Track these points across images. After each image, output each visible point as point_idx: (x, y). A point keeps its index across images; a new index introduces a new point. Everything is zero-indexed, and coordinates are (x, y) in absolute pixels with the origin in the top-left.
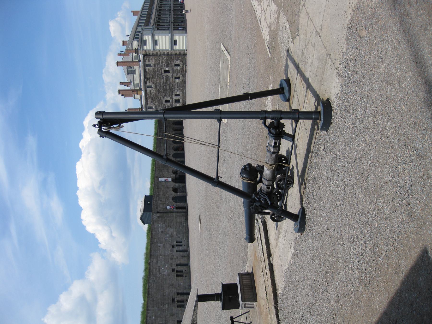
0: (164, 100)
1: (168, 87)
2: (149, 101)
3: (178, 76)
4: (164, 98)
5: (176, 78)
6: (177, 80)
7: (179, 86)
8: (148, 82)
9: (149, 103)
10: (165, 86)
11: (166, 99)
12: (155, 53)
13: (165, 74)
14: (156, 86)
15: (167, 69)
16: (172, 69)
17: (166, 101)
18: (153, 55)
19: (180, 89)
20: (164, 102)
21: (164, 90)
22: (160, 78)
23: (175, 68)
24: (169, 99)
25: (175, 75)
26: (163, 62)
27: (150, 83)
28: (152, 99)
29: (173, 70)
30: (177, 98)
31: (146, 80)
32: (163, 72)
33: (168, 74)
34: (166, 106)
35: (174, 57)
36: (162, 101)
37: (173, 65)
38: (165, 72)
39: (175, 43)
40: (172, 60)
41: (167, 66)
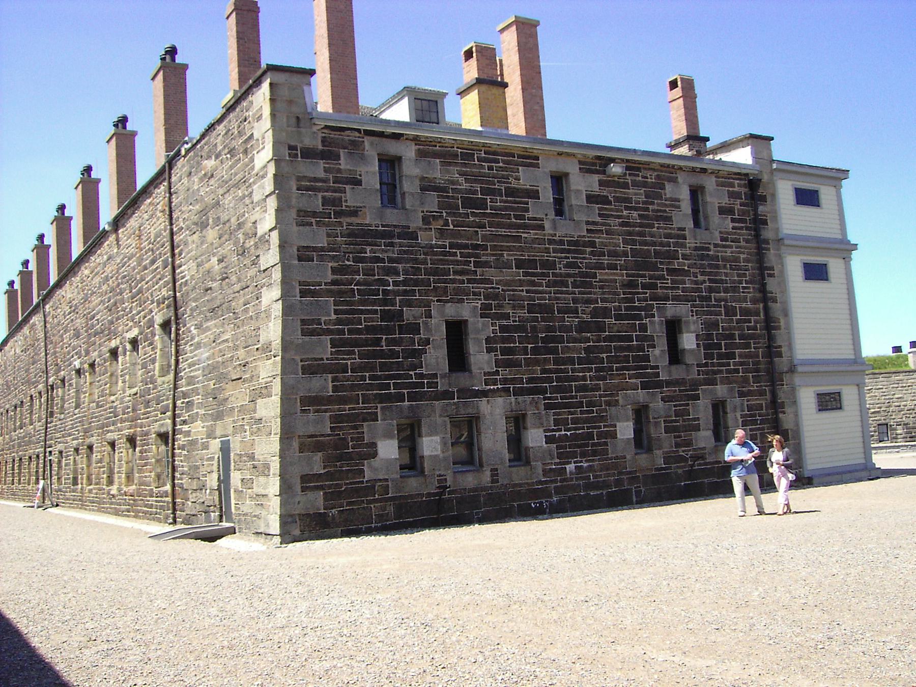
0: (466, 311)
1: (577, 350)
2: (454, 173)
3: (658, 432)
4: (485, 312)
5: (640, 414)
6: (625, 430)
7: (586, 441)
8: (592, 183)
9: (437, 171)
10: (583, 327)
11: (480, 330)
12: (771, 256)
13: (656, 327)
14: (576, 245)
15: (688, 341)
16: (695, 385)
17: (457, 332)
18: (760, 245)
19: (565, 457)
20: (451, 311)
21: (546, 309)
22: (631, 285)
23: (702, 410)
24: (481, 359)
25: (658, 406)
26: (730, 312)
27: (591, 199)
28: (469, 203)
29: (688, 392)
30: (494, 439)
31: (616, 169)
32: (673, 309)
33: (658, 353)
34: (414, 329)
35: (762, 393)
36: (459, 297)
37: (721, 390)
38: (673, 328)
39: (829, 402)
40: (745, 380)
41: (707, 342)
